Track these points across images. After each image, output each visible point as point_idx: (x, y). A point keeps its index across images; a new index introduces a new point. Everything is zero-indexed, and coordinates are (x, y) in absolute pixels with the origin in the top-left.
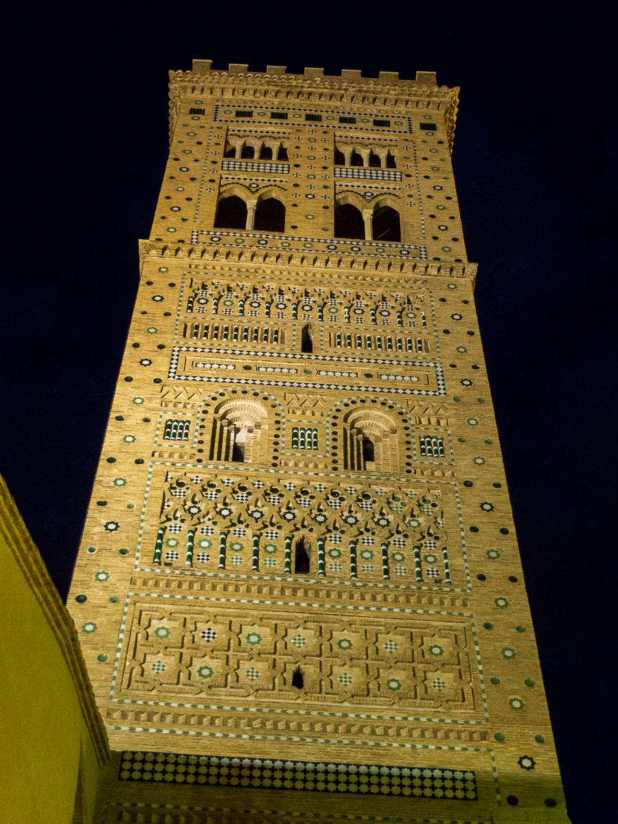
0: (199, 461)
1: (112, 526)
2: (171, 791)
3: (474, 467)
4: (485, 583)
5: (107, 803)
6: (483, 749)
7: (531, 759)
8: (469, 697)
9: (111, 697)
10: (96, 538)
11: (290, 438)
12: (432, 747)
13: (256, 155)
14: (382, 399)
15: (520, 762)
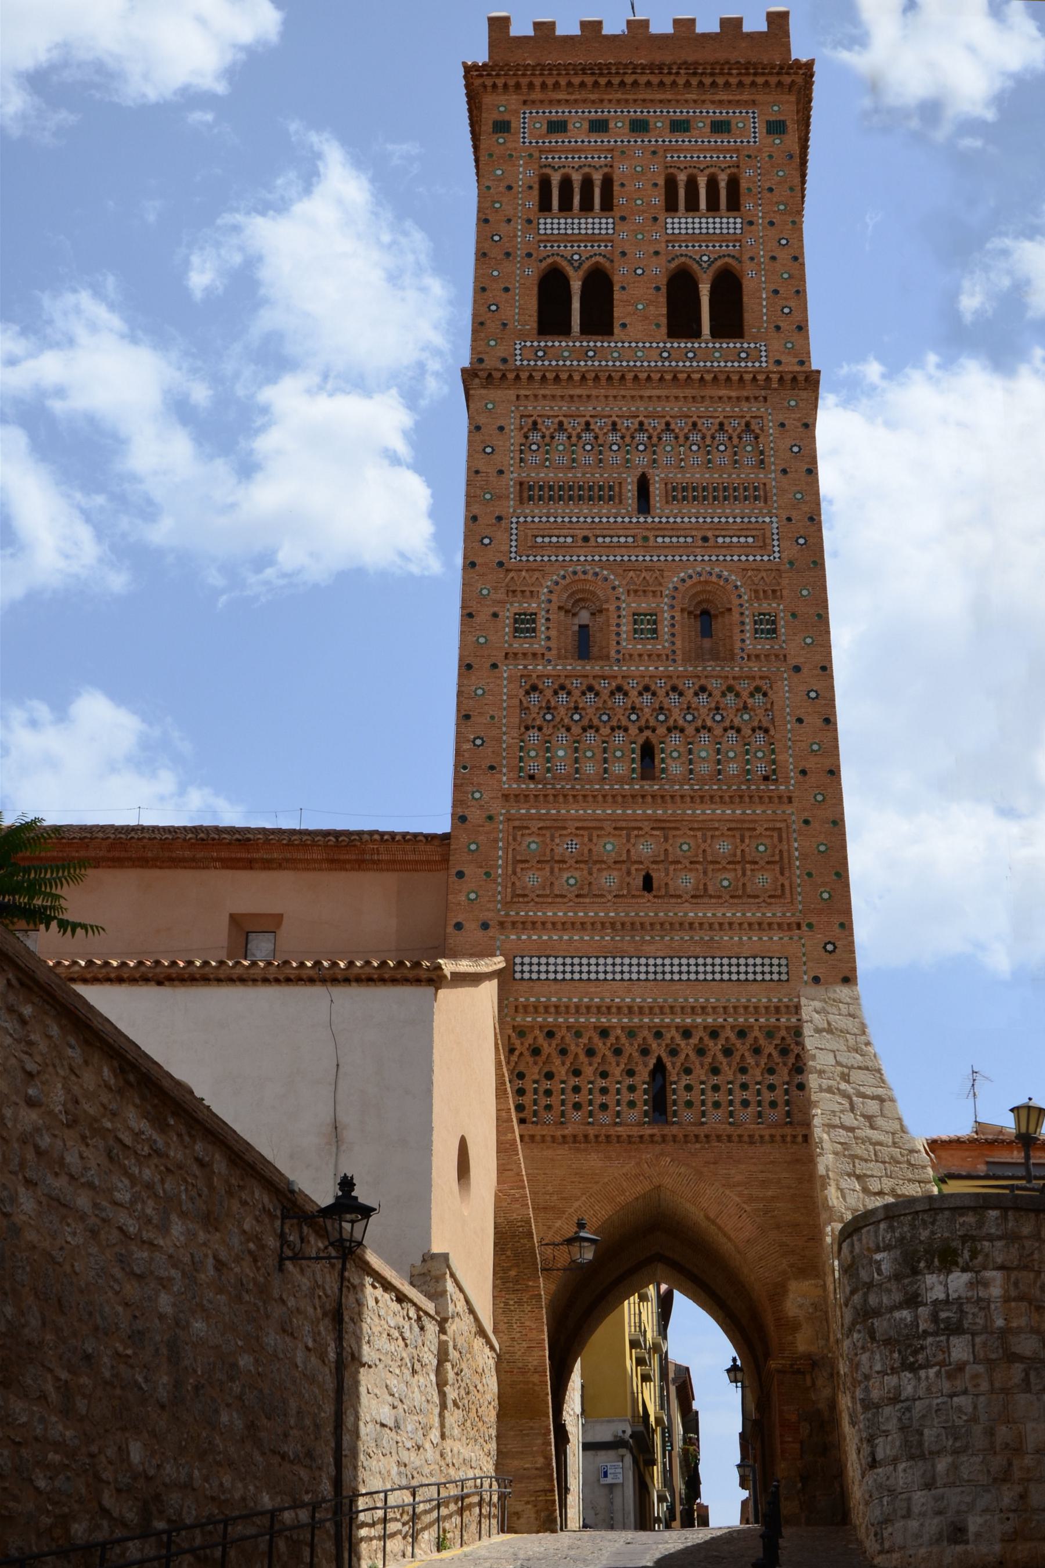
0: (549, 661)
1: (478, 742)
2: (554, 987)
3: (803, 648)
6: (796, 938)
8: (787, 892)
10: (466, 755)
12: (755, 938)
14: (717, 570)
15: (824, 947)
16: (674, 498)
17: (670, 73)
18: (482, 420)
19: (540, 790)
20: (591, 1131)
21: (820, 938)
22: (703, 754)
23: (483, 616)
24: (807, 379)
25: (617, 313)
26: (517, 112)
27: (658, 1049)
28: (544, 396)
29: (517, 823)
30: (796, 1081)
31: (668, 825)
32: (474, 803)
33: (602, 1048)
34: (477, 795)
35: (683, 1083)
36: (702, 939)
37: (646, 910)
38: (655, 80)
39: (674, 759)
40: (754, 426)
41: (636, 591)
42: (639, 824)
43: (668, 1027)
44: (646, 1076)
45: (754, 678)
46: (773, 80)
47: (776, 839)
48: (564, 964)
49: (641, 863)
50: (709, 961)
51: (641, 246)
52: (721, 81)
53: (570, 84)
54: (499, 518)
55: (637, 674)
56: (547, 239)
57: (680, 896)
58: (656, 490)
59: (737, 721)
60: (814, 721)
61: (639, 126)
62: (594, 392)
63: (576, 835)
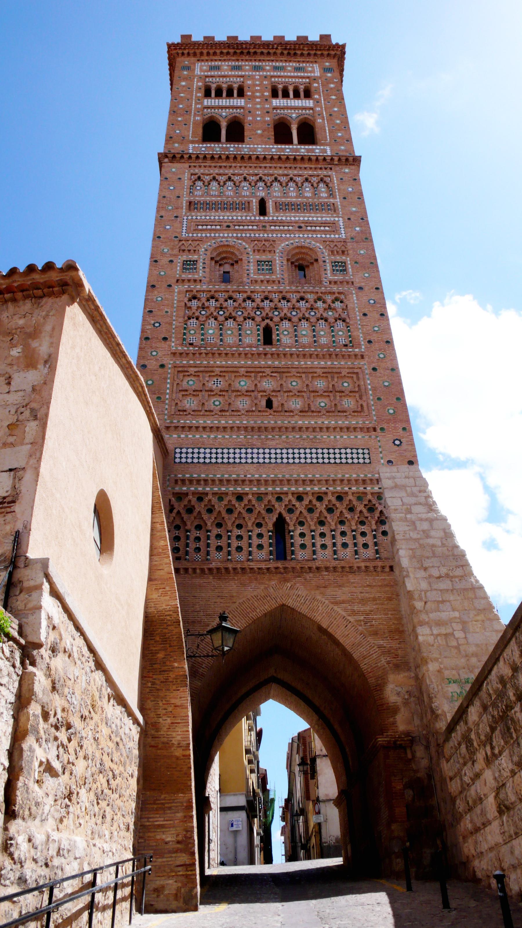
1: (157, 325)
2: (203, 467)
4: (372, 344)
5: (169, 476)
6: (373, 437)
7: (400, 440)
9: (166, 420)
10: (149, 332)
11: (256, 267)
13: (224, 94)
15: (394, 442)
16: (280, 209)
17: (273, 48)
18: (168, 176)
19: (197, 350)
20: (230, 566)
21: (390, 437)
22: (304, 333)
23: (164, 261)
24: (354, 160)
25: (246, 134)
26: (194, 64)
27: (280, 508)
28: (205, 167)
29: (180, 369)
30: (381, 530)
31: (282, 370)
32: (152, 357)
33: (239, 507)
34: (154, 353)
35: (298, 532)
36: (308, 437)
37: (270, 420)
38: (265, 51)
39: (285, 335)
40: (326, 179)
41: (259, 251)
42: (263, 370)
43: (286, 493)
44: (271, 527)
45: (334, 293)
46: (326, 53)
47: (355, 379)
48: (211, 453)
49: (265, 392)
50: (314, 451)
51: (258, 111)
52: (299, 52)
53: (222, 53)
54: (176, 217)
55: (260, 290)
56: (208, 108)
57: (292, 411)
58: (270, 206)
59: (325, 315)
60: (374, 315)
61: (256, 69)
62: (233, 165)
63: (220, 376)
